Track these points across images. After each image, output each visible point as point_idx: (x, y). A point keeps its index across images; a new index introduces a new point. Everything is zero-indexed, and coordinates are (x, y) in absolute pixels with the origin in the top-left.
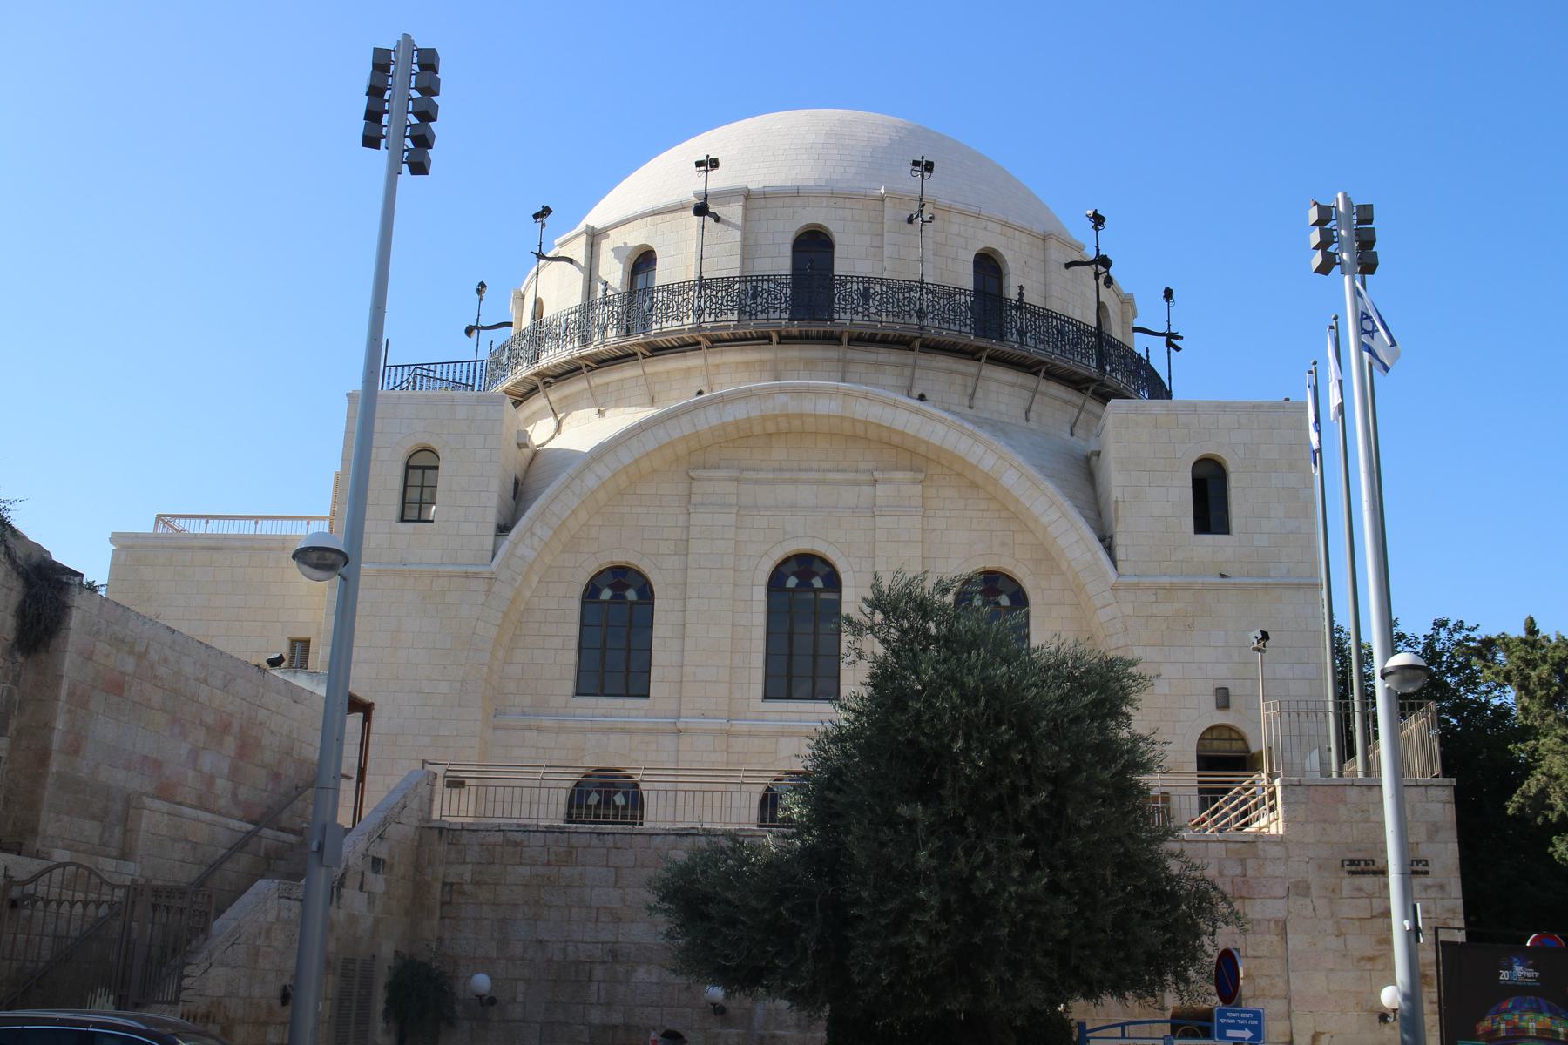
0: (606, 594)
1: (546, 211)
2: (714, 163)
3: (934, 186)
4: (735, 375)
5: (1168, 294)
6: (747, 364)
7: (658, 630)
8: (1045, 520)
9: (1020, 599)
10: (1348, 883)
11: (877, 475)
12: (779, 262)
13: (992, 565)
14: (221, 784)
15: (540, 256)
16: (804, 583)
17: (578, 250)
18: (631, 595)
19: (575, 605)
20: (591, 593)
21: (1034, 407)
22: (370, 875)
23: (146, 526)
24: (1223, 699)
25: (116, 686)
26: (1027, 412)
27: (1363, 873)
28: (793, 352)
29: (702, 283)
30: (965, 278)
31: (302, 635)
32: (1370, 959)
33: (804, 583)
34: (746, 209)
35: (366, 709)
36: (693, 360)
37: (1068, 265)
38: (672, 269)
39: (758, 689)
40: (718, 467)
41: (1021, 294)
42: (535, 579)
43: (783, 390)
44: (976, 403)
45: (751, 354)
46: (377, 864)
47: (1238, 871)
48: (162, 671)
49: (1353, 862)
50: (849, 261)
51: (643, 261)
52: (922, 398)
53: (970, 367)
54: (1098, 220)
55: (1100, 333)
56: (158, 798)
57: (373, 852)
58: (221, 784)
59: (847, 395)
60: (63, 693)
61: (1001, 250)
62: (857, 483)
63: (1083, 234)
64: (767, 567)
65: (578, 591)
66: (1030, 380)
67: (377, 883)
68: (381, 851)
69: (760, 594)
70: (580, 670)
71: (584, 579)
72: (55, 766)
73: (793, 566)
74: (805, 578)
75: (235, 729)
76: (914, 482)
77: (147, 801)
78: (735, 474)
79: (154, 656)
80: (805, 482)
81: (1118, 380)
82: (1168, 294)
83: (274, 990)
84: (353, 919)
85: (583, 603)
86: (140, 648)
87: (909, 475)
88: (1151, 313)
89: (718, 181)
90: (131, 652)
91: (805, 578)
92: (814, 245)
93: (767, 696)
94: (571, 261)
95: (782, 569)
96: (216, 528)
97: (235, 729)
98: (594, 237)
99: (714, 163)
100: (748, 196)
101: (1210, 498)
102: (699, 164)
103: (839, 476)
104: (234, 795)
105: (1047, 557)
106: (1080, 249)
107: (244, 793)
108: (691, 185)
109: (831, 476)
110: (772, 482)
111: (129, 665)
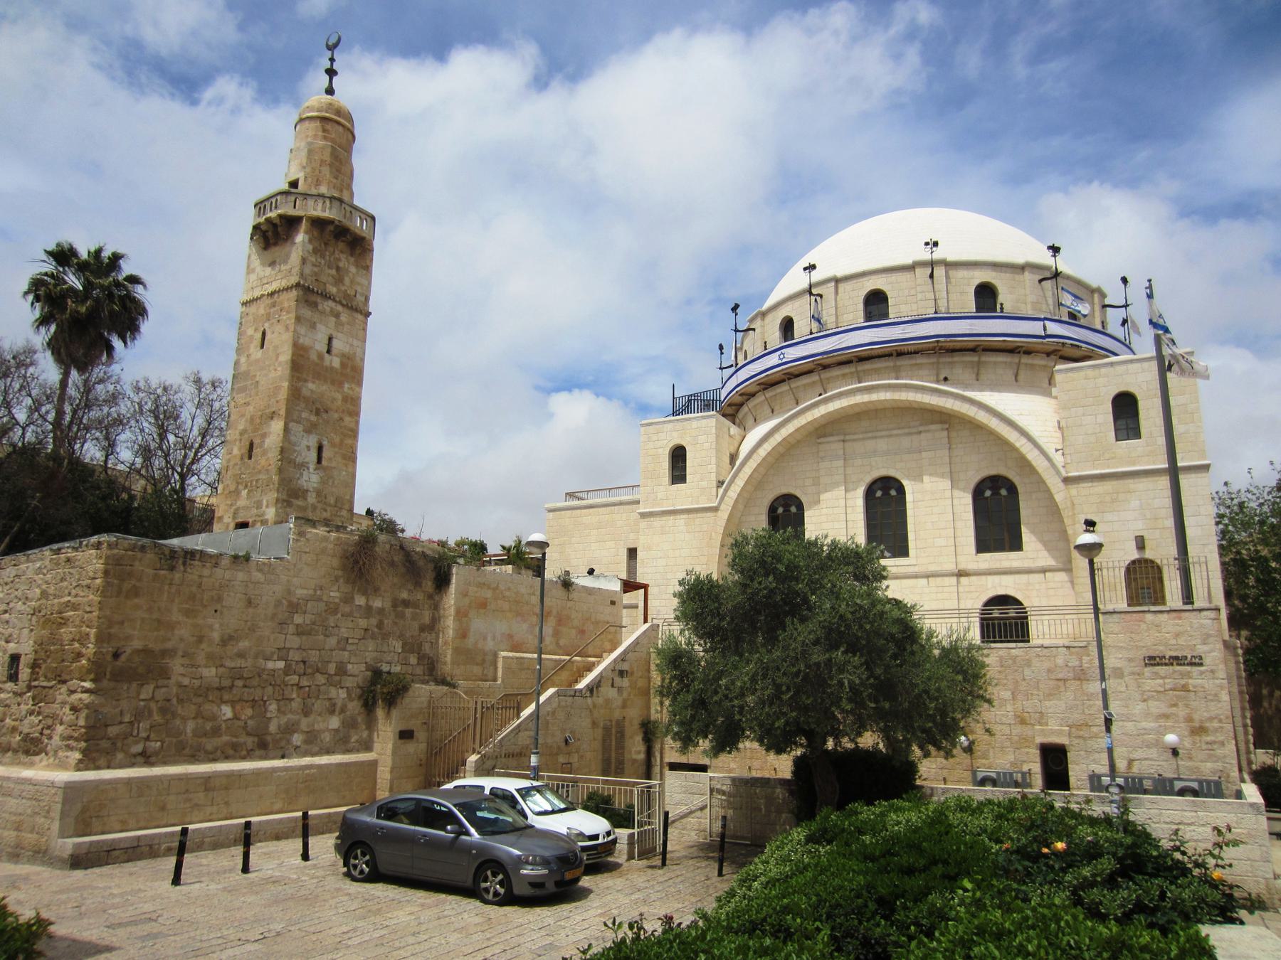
2: (813, 267)
5: (1124, 280)
6: (844, 375)
8: (1017, 445)
9: (1013, 489)
10: (1148, 670)
13: (993, 472)
15: (736, 331)
16: (886, 493)
18: (793, 509)
20: (772, 510)
22: (618, 680)
24: (1141, 543)
25: (483, 605)
27: (1158, 664)
32: (1166, 716)
33: (886, 493)
35: (645, 587)
37: (1040, 281)
40: (832, 435)
41: (1002, 309)
42: (741, 507)
44: (982, 377)
47: (1077, 663)
48: (507, 594)
49: (1151, 658)
52: (946, 379)
57: (619, 667)
61: (993, 281)
66: (1014, 359)
67: (625, 682)
68: (625, 666)
73: (879, 484)
74: (886, 492)
75: (554, 612)
78: (842, 437)
79: (502, 587)
80: (882, 437)
82: (1124, 280)
83: (559, 739)
84: (608, 701)
86: (494, 586)
87: (938, 426)
89: (816, 276)
90: (489, 588)
91: (886, 492)
95: (875, 487)
97: (554, 612)
99: (813, 267)
102: (805, 269)
103: (899, 432)
104: (557, 643)
106: (1047, 268)
107: (562, 642)
109: (895, 432)
110: (864, 439)
111: (489, 594)
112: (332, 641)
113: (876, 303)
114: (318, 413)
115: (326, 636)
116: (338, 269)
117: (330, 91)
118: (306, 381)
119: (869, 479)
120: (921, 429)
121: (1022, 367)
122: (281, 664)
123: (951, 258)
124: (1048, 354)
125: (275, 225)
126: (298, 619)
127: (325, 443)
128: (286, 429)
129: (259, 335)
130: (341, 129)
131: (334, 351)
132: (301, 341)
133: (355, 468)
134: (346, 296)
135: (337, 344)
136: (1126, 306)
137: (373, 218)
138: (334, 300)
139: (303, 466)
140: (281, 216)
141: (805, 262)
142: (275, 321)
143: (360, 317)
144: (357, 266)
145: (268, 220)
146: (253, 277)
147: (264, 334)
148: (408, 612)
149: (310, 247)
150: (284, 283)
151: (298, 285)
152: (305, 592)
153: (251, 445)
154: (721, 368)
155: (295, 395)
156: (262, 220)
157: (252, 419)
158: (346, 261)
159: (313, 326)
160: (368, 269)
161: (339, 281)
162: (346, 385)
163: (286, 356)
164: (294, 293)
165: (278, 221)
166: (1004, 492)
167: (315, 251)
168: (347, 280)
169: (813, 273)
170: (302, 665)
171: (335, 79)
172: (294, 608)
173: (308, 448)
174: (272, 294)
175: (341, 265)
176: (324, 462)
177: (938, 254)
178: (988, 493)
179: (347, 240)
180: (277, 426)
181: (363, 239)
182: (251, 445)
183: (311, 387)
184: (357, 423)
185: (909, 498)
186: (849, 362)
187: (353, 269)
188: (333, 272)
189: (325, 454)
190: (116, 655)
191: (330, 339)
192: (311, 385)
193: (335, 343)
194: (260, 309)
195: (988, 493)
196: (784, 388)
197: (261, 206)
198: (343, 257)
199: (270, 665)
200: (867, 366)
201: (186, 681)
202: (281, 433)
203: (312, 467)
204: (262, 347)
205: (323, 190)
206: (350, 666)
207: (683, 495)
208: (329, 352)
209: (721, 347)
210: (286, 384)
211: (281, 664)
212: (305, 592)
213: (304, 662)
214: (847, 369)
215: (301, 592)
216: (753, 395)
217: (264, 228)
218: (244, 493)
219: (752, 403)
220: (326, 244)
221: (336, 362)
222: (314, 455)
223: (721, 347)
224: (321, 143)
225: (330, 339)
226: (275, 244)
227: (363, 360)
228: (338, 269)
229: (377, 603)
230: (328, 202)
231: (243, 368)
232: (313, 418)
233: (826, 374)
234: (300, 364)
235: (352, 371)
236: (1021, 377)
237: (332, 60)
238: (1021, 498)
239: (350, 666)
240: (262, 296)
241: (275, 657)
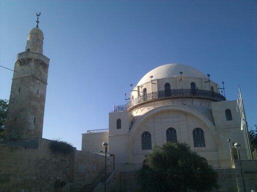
2: (152, 77)
3: (183, 75)
4: (159, 104)
9: (202, 132)
12: (163, 89)
14: (95, 170)
17: (137, 89)
23: (85, 132)
28: (166, 101)
29: (152, 93)
30: (189, 87)
38: (149, 91)
45: (160, 102)
46: (115, 178)
49: (246, 172)
50: (172, 88)
51: (145, 90)
54: (209, 75)
55: (213, 92)
69: (165, 134)
81: (216, 98)
89: (153, 79)
92: (167, 85)
98: (138, 87)
99: (152, 77)
100: (158, 80)
101: (228, 114)
117: (37, 26)
119: (167, 128)
122: (36, 177)
125: (24, 60)
135: (40, 92)
160: (47, 72)
161: (40, 75)
167: (35, 67)
178: (196, 132)
187: (44, 73)
189: (36, 120)
197: (20, 55)
205: (37, 52)
207: (120, 131)
211: (36, 177)
222: (33, 120)
231: (13, 97)
237: (38, 19)
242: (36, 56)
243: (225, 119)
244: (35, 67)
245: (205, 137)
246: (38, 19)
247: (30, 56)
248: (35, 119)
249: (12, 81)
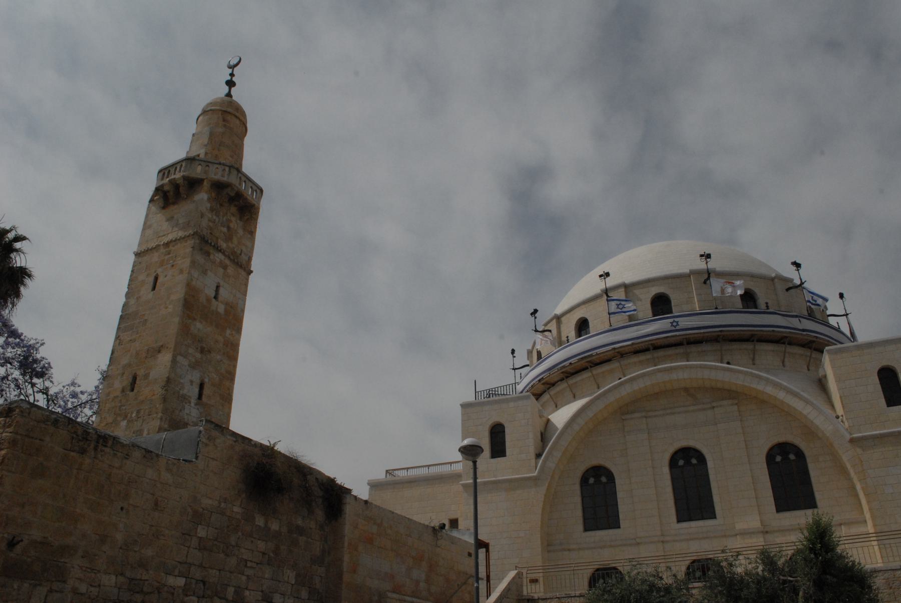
0: (592, 480)
1: (536, 311)
2: (607, 274)
5: (841, 296)
6: (640, 362)
7: (620, 495)
8: (805, 412)
9: (800, 454)
11: (714, 404)
13: (781, 439)
14: (422, 585)
15: (536, 331)
16: (688, 462)
18: (604, 479)
19: (577, 487)
20: (584, 480)
21: (786, 360)
26: (783, 362)
31: (453, 517)
33: (688, 462)
34: (626, 292)
36: (614, 365)
37: (788, 290)
39: (674, 518)
43: (660, 371)
52: (728, 363)
53: (749, 346)
54: (797, 265)
56: (394, 592)
58: (422, 585)
59: (691, 367)
60: (346, 544)
61: (753, 288)
62: (704, 409)
63: (790, 273)
64: (667, 457)
65: (578, 481)
66: (781, 348)
69: (666, 470)
70: (585, 519)
71: (579, 474)
72: (346, 577)
76: (732, 405)
77: (389, 594)
78: (644, 414)
82: (841, 296)
85: (581, 486)
88: (834, 306)
89: (610, 282)
93: (679, 521)
94: (550, 331)
96: (412, 473)
98: (558, 318)
99: (607, 274)
100: (626, 287)
102: (601, 276)
105: (810, 432)
106: (791, 280)
108: (598, 286)
109: (691, 408)
112: (233, 561)
113: (661, 304)
114: (202, 351)
115: (227, 555)
116: (229, 228)
118: (195, 319)
119: (672, 450)
120: (714, 404)
121: (787, 355)
122: (181, 582)
123: (718, 269)
124: (803, 346)
126: (202, 532)
127: (206, 380)
128: (174, 361)
129: (151, 279)
130: (238, 122)
131: (220, 298)
132: (194, 283)
133: (230, 408)
134: (234, 253)
136: (847, 315)
137: (262, 191)
138: (224, 253)
139: (184, 399)
140: (184, 178)
141: (600, 270)
142: (169, 266)
143: (243, 273)
144: (244, 230)
145: (173, 183)
146: (149, 232)
147: (156, 279)
148: (302, 539)
149: (209, 205)
150: (181, 234)
151: (195, 233)
152: (210, 502)
153: (135, 379)
154: (514, 369)
155: (185, 330)
156: (166, 181)
157: (137, 354)
158: (236, 223)
159: (205, 272)
160: (252, 233)
161: (229, 238)
162: (228, 332)
163: (179, 294)
164: (191, 242)
165: (181, 182)
166: (792, 457)
167: (212, 210)
168: (235, 240)
169: (608, 279)
170: (201, 585)
171: (233, 89)
172: (198, 517)
173: (192, 382)
174: (167, 245)
175: (232, 225)
176: (204, 399)
177: (713, 264)
178: (779, 459)
179: (239, 203)
180: (165, 358)
181: (253, 205)
182: (135, 379)
183: (199, 327)
184: (235, 367)
185: (710, 464)
186: (647, 350)
188: (225, 230)
189: (207, 391)
190: (12, 544)
191: (218, 287)
192: (199, 325)
193: (221, 291)
194: (155, 257)
195: (779, 459)
196: (586, 375)
197: (164, 172)
198: (233, 219)
199: (171, 581)
200: (661, 353)
201: (83, 588)
202: (169, 364)
203: (193, 401)
204: (154, 288)
206: (247, 593)
208: (216, 298)
209: (513, 351)
210: (176, 320)
211: (181, 582)
212: (210, 502)
213: (204, 583)
214: (642, 357)
215: (206, 502)
216: (553, 385)
217: (166, 188)
218: (124, 423)
219: (553, 391)
220: (221, 205)
221: (221, 309)
222: (197, 390)
223: (513, 351)
224: (220, 130)
225: (218, 287)
226: (174, 203)
227: (243, 311)
228: (229, 228)
229: (275, 526)
230: (227, 169)
232: (198, 355)
233: (625, 362)
234: (192, 305)
235: (232, 320)
236: (787, 363)
237: (232, 75)
238: (809, 460)
239: (247, 593)
240: (158, 246)
241: (176, 573)
242: (217, 174)
243: (883, 401)
244: (212, 210)
245: (812, 473)
246: (232, 75)
247: (198, 171)
248: (202, 386)
249: (132, 258)
